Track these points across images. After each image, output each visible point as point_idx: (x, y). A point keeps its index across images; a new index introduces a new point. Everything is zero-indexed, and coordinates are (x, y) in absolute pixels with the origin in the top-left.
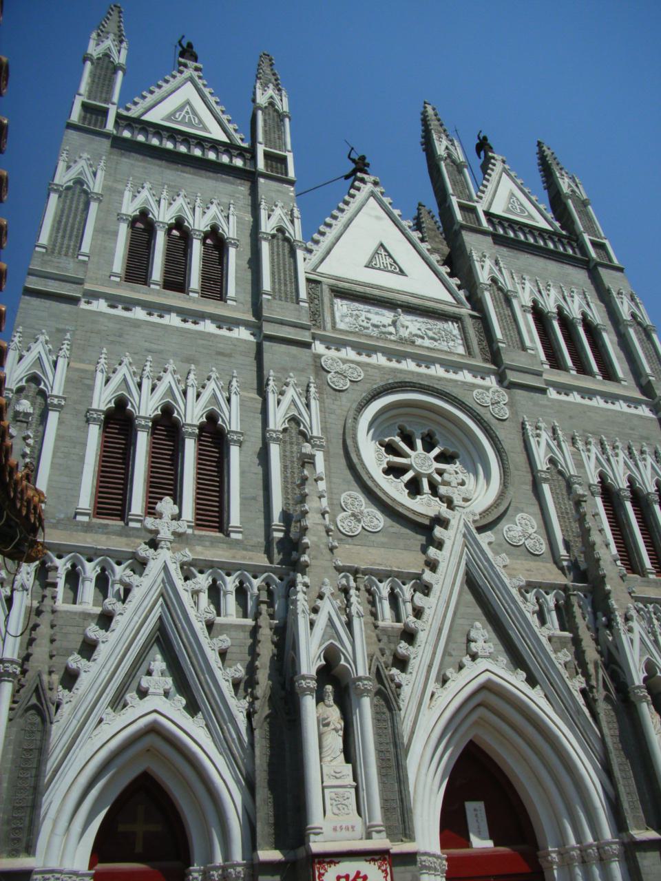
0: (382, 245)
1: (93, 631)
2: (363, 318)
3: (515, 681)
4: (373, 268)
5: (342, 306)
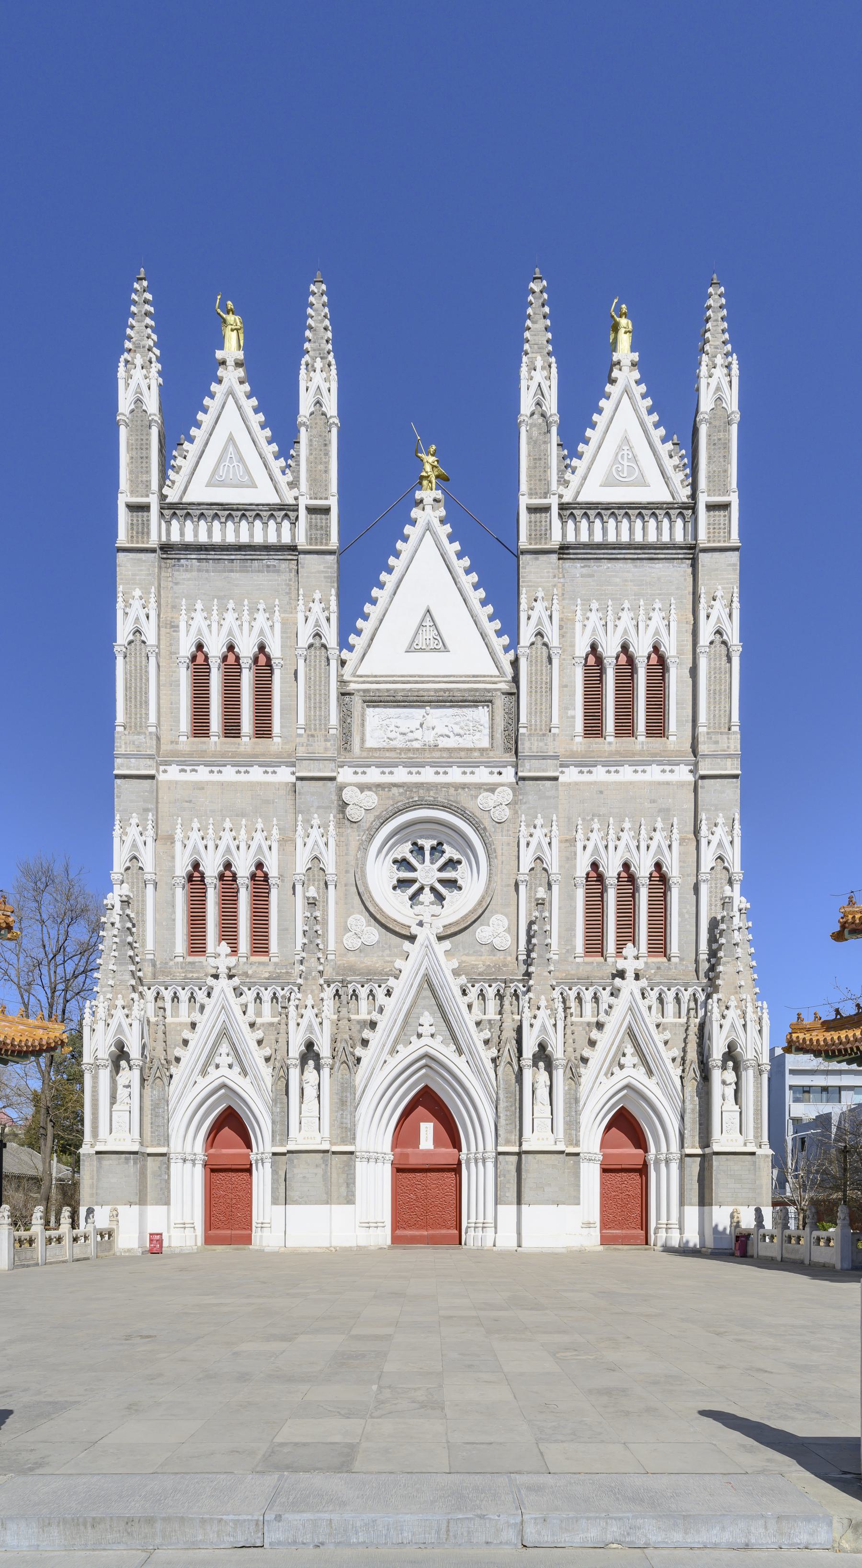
0: (428, 611)
1: (187, 1034)
2: (392, 728)
4: (416, 650)
5: (375, 716)
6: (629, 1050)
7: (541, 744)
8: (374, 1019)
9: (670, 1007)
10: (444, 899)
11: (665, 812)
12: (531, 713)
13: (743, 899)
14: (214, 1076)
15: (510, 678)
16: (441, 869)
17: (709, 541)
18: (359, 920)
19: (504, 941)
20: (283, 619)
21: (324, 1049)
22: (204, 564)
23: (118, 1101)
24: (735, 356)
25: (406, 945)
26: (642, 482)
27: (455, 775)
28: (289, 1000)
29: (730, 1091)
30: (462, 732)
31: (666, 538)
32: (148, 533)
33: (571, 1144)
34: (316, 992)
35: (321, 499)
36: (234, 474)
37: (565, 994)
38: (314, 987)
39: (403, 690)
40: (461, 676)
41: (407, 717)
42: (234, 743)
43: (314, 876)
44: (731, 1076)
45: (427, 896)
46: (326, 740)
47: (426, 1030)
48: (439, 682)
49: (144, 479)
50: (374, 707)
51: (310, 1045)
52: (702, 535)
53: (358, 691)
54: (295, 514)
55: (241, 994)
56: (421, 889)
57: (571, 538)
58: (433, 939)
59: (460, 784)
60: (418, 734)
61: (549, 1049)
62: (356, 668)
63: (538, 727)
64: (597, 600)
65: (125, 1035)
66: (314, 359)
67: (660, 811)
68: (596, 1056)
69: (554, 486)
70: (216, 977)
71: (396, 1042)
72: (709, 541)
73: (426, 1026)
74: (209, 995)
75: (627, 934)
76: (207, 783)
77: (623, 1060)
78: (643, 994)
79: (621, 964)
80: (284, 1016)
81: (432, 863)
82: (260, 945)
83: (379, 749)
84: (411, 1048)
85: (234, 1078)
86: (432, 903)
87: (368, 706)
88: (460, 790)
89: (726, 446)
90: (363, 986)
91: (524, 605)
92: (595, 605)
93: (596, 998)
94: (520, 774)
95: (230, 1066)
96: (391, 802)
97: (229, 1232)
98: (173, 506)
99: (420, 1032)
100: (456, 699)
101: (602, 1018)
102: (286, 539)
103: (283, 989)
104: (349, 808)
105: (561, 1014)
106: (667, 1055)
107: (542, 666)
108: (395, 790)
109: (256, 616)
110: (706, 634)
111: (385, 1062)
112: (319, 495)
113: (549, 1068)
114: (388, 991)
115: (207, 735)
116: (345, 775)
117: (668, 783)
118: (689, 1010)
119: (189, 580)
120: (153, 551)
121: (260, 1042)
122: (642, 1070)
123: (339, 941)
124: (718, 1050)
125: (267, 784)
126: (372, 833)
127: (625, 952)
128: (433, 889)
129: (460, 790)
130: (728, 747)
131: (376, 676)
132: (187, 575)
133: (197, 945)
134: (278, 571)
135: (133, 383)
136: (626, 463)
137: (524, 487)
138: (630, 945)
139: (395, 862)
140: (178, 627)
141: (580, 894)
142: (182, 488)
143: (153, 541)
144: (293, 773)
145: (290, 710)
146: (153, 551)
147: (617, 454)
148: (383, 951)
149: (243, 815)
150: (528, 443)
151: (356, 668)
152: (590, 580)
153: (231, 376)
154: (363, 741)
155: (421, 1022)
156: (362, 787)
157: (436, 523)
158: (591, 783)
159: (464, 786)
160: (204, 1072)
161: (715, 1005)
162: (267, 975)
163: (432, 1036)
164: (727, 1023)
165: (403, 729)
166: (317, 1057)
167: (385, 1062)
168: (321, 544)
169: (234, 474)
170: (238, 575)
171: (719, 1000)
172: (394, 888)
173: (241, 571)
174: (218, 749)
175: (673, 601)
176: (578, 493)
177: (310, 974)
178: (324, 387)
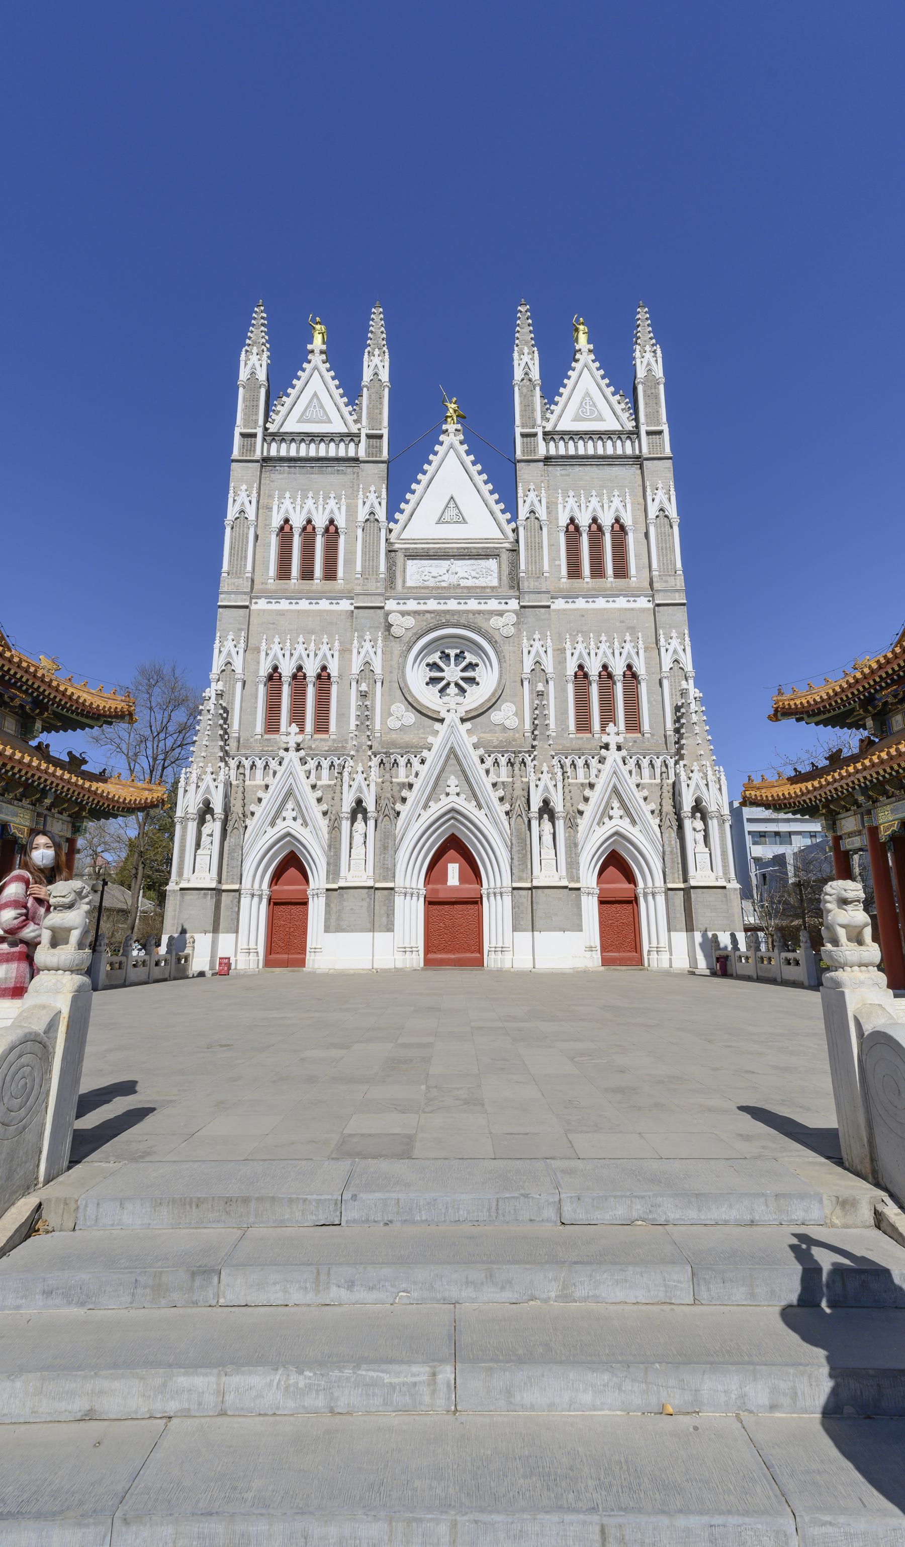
1: (260, 794)
3: (468, 807)
4: (443, 523)
5: (413, 566)
6: (616, 804)
7: (536, 583)
8: (411, 781)
9: (646, 771)
10: (466, 692)
11: (632, 630)
12: (528, 563)
13: (697, 690)
14: (281, 827)
15: (512, 540)
16: (463, 670)
17: (650, 454)
18: (399, 708)
19: (513, 722)
20: (347, 503)
21: (370, 805)
22: (293, 469)
23: (202, 847)
24: (658, 346)
25: (437, 726)
26: (600, 418)
27: (473, 605)
28: (344, 767)
29: (700, 836)
30: (477, 576)
32: (254, 451)
33: (573, 881)
34: (365, 761)
36: (317, 415)
37: (562, 762)
38: (364, 758)
39: (434, 548)
40: (476, 539)
41: (437, 566)
42: (309, 584)
43: (365, 675)
44: (699, 825)
45: (452, 690)
46: (376, 582)
47: (453, 790)
48: (460, 543)
49: (254, 418)
50: (412, 559)
51: (359, 802)
52: (645, 450)
53: (401, 549)
54: (358, 439)
55: (306, 763)
56: (448, 684)
57: (553, 452)
58: (458, 721)
59: (477, 611)
60: (445, 577)
61: (552, 804)
62: (400, 534)
63: (534, 572)
65: (211, 795)
66: (374, 349)
67: (628, 628)
68: (589, 810)
69: (539, 421)
70: (287, 750)
71: (429, 799)
73: (453, 787)
74: (280, 764)
75: (608, 716)
76: (287, 611)
77: (611, 813)
78: (624, 761)
79: (605, 739)
80: (339, 779)
81: (456, 665)
82: (322, 726)
83: (416, 587)
84: (440, 804)
85: (297, 828)
86: (456, 695)
87: (408, 559)
88: (477, 615)
89: (657, 397)
90: (402, 757)
92: (571, 493)
93: (587, 765)
94: (521, 604)
95: (295, 819)
96: (425, 624)
97: (286, 956)
98: (273, 435)
99: (448, 791)
100: (473, 554)
101: (593, 780)
102: (352, 453)
103: (339, 759)
104: (393, 627)
105: (559, 776)
106: (646, 808)
107: (535, 532)
108: (428, 615)
109: (328, 501)
110: (653, 511)
111: (420, 815)
112: (375, 428)
113: (552, 819)
114: (422, 760)
116: (391, 605)
117: (632, 609)
118: (661, 774)
119: (281, 479)
120: (257, 461)
121: (319, 800)
122: (627, 820)
123: (384, 722)
124: (687, 804)
128: (457, 685)
129: (477, 615)
131: (414, 539)
132: (281, 476)
133: (272, 725)
134: (345, 474)
135: (250, 364)
136: (588, 407)
137: (518, 421)
138: (611, 724)
139: (428, 665)
140: (272, 508)
141: (570, 688)
142: (280, 423)
143: (258, 455)
144: (352, 604)
145: (350, 562)
146: (257, 461)
149: (313, 633)
150: (520, 396)
151: (400, 534)
152: (567, 478)
153: (317, 359)
154: (404, 582)
155: (448, 783)
156: (403, 614)
157: (457, 444)
158: (575, 610)
159: (479, 612)
160: (273, 824)
161: (682, 769)
162: (327, 748)
163: (458, 794)
164: (693, 784)
165: (432, 575)
166: (365, 812)
167: (420, 815)
168: (376, 457)
169: (317, 415)
171: (685, 765)
172: (427, 684)
174: (296, 588)
175: (627, 490)
176: (556, 425)
177: (361, 747)
178: (380, 365)
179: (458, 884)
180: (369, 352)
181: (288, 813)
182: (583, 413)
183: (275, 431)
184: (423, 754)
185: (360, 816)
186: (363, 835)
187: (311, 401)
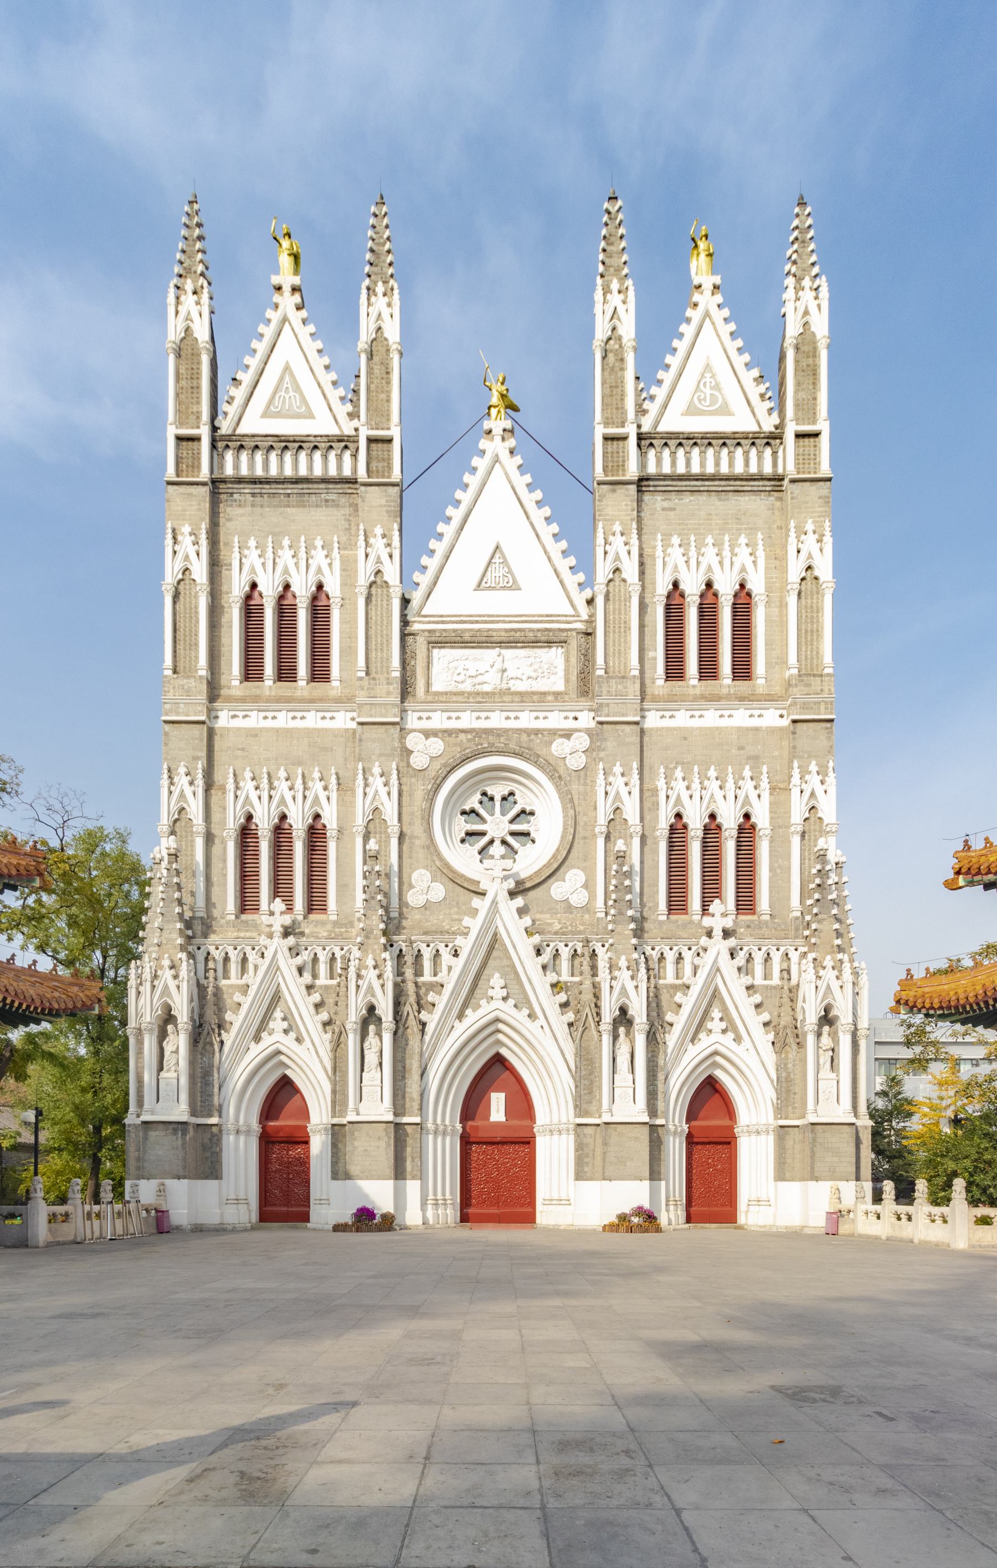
7: (620, 687)
11: (755, 761)
13: (839, 852)
17: (798, 473)
19: (579, 899)
22: (258, 499)
23: (165, 1068)
24: (824, 278)
26: (725, 410)
28: (349, 960)
30: (534, 675)
31: (753, 469)
32: (199, 467)
34: (378, 952)
35: (383, 429)
36: (290, 405)
37: (647, 953)
38: (376, 947)
39: (471, 630)
40: (534, 616)
41: (475, 659)
42: (290, 688)
43: (375, 828)
45: (497, 849)
46: (388, 684)
48: (510, 622)
49: (195, 410)
50: (440, 648)
53: (423, 631)
54: (355, 445)
55: (298, 954)
56: (491, 842)
57: (652, 469)
59: (533, 730)
61: (630, 1013)
63: (617, 669)
64: (679, 535)
65: (171, 998)
67: (749, 758)
69: (631, 414)
71: (465, 1006)
72: (798, 473)
73: (497, 988)
75: (711, 890)
76: (261, 729)
78: (732, 954)
80: (343, 978)
81: (503, 813)
82: (315, 903)
83: (446, 693)
84: (480, 1012)
85: (287, 1043)
86: (503, 857)
87: (433, 647)
88: (533, 736)
90: (428, 946)
91: (600, 540)
95: (286, 1032)
96: (459, 749)
97: (285, 1209)
100: (528, 639)
103: (342, 949)
107: (620, 605)
108: (462, 737)
112: (381, 426)
115: (260, 678)
117: (756, 729)
119: (242, 515)
120: (204, 484)
121: (318, 1006)
125: (326, 730)
126: (438, 782)
127: (712, 909)
128: (504, 842)
129: (533, 736)
130: (822, 690)
131: (442, 616)
132: (240, 511)
134: (338, 506)
136: (708, 391)
137: (598, 416)
140: (230, 565)
142: (236, 419)
144: (353, 719)
145: (348, 651)
146: (204, 484)
147: (699, 382)
148: (450, 909)
149: (299, 763)
152: (672, 513)
154: (428, 684)
155: (491, 984)
156: (427, 734)
158: (675, 729)
159: (537, 732)
160: (257, 1039)
162: (325, 934)
168: (383, 477)
169: (290, 405)
170: (294, 510)
173: (298, 506)
174: (273, 694)
176: (657, 423)
177: (372, 932)
179: (503, 1119)
180: (368, 289)
181: (277, 1024)
182: (700, 400)
183: (229, 432)
184: (457, 943)
185: (372, 1028)
186: (378, 1054)
187: (281, 379)
